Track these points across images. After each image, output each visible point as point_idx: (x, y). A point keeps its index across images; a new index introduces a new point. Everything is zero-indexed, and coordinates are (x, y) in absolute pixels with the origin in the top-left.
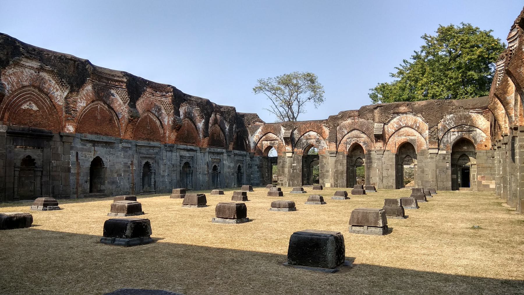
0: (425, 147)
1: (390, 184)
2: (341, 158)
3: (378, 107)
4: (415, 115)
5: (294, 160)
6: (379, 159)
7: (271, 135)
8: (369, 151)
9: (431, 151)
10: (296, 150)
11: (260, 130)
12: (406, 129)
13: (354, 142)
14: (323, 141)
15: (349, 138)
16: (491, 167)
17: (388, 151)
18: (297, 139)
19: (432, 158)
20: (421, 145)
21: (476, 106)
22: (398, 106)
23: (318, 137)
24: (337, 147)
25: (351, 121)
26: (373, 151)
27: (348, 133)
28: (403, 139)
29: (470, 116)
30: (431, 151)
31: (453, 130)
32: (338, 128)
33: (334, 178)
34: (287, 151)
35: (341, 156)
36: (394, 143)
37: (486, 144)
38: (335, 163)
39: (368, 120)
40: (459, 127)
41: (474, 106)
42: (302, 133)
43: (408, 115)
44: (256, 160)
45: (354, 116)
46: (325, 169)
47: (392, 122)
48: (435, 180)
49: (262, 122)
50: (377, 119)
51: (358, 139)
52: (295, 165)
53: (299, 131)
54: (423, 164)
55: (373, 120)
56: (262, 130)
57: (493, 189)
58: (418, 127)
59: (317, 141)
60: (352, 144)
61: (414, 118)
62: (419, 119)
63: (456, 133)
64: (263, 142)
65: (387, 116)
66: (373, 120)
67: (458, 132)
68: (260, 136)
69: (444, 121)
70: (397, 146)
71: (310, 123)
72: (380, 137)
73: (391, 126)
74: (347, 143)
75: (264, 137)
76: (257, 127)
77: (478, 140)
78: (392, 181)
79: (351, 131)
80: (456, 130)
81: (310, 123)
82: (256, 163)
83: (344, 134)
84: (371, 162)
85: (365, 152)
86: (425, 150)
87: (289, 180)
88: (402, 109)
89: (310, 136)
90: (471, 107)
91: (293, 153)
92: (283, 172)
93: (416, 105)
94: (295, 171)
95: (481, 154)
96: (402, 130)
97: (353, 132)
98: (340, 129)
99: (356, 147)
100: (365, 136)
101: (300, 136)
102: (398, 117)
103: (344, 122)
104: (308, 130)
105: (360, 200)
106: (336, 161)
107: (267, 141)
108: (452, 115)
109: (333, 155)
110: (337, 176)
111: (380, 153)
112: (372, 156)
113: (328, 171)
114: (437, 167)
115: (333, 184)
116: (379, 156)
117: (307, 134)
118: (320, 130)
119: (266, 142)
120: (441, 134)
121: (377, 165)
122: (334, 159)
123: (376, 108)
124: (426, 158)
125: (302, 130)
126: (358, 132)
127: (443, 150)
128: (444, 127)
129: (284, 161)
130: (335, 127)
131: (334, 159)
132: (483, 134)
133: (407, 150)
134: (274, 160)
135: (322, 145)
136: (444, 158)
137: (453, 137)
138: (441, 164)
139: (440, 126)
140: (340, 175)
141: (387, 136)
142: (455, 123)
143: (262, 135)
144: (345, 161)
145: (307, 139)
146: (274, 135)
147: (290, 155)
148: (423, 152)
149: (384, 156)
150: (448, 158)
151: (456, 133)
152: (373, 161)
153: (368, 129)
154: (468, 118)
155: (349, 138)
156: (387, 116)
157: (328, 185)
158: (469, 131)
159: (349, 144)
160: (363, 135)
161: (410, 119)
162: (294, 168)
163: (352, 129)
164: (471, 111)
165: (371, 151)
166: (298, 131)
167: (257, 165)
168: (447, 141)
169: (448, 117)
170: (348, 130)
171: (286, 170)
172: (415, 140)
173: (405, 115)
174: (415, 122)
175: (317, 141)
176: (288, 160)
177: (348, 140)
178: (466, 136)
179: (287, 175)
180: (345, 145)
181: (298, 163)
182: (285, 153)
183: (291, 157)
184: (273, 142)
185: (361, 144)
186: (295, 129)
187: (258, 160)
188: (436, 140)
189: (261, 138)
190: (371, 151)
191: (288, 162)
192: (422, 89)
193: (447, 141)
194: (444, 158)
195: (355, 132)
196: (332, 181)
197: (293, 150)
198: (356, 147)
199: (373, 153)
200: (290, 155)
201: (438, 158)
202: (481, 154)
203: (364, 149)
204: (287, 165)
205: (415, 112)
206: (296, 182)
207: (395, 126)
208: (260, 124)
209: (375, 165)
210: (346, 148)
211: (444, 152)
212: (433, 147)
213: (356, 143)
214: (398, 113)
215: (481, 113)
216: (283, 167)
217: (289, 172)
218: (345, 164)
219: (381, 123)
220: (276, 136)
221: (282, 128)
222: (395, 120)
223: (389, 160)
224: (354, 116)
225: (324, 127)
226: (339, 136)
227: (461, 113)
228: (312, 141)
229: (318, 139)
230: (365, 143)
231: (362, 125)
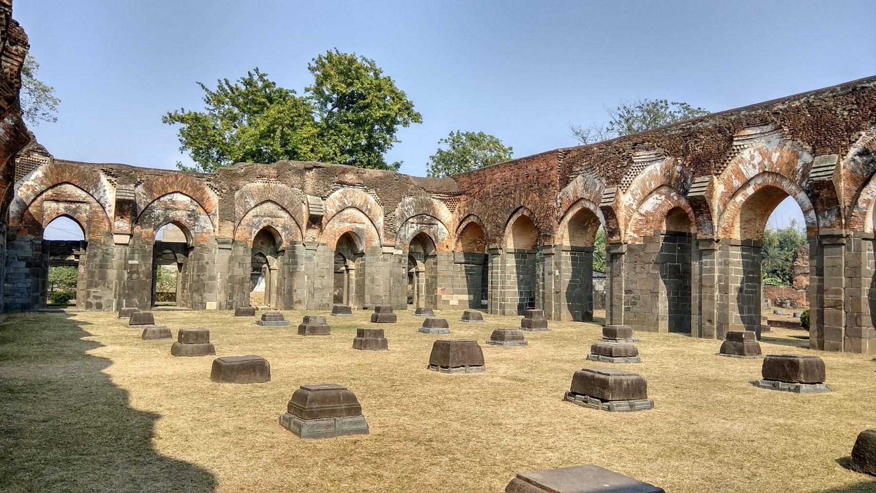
0: (376, 243)
1: (325, 301)
2: (241, 253)
3: (315, 167)
4: (366, 191)
5: (133, 252)
6: (310, 258)
7: (69, 189)
8: (293, 243)
9: (386, 250)
10: (137, 229)
11: (39, 173)
12: (352, 210)
13: (265, 224)
14: (203, 217)
15: (257, 216)
16: (452, 277)
17: (324, 244)
18: (143, 207)
19: (385, 260)
20: (371, 240)
21: (440, 190)
22: (344, 172)
23: (192, 207)
24: (234, 231)
25: (262, 184)
26: (300, 243)
27: (256, 206)
28: (346, 227)
29: (432, 203)
30: (386, 250)
31: (411, 220)
32: (237, 194)
33: (226, 292)
34: (116, 230)
35: (241, 249)
36: (335, 229)
37: (447, 244)
38: (229, 262)
39: (292, 187)
40: (420, 216)
41: (438, 189)
42: (156, 195)
43: (356, 190)
44: (22, 248)
45: (269, 177)
46: (207, 273)
47: (332, 196)
48: (388, 293)
49: (46, 154)
50: (309, 189)
51: (274, 220)
52: (136, 262)
53: (149, 189)
54: (374, 269)
55: (302, 188)
56: (46, 175)
57: (453, 307)
58: (370, 211)
59: (189, 216)
60: (261, 227)
61: (365, 194)
62: (371, 199)
63: (414, 225)
64: (46, 204)
65: (327, 186)
66: (302, 188)
67: (417, 224)
68: (38, 189)
69: (403, 206)
70: (337, 238)
71: (176, 176)
72: (315, 221)
73: (331, 204)
74: (252, 225)
75: (50, 192)
76: (33, 166)
77: (440, 238)
78: (328, 297)
79: (262, 203)
80: (415, 220)
81: (176, 176)
82: (21, 254)
83: (248, 207)
84: (296, 263)
85: (285, 245)
86: (376, 247)
87: (119, 296)
88: (350, 177)
89: (174, 202)
90: (435, 190)
91: (131, 236)
92: (103, 277)
93: (366, 175)
94: (135, 276)
95: (442, 258)
96: (346, 212)
97: (265, 206)
98: (242, 196)
99: (268, 236)
100: (286, 215)
101: (149, 201)
102: (341, 190)
103: (250, 185)
104: (170, 190)
105: (462, 332)
106: (231, 259)
107: (57, 201)
108: (411, 198)
109: (225, 246)
110: (232, 288)
111: (313, 247)
112: (297, 253)
113: (213, 278)
114: (391, 275)
115: (224, 304)
116: (309, 253)
117: (168, 197)
118: (198, 194)
119: (54, 205)
120: (398, 224)
121: (307, 269)
122: (227, 254)
123: (310, 169)
124: (378, 259)
125: (155, 189)
126: (274, 206)
127: (399, 249)
128: (403, 215)
129: (106, 255)
130: (232, 192)
131: (227, 254)
132: (445, 230)
133: (348, 243)
134: (63, 250)
135: (203, 224)
136: (400, 262)
137: (411, 230)
138: (396, 270)
139: (397, 213)
140: (237, 286)
141: (324, 220)
142: (415, 211)
143: (44, 187)
144: (248, 260)
145: (167, 209)
146: (79, 192)
147: (126, 239)
148: (374, 251)
149: (317, 253)
150: (405, 261)
151: (414, 225)
152: (299, 261)
153: (292, 203)
154: (430, 205)
155: (257, 216)
156: (327, 186)
157: (211, 305)
158: (430, 224)
159: (257, 228)
160: (282, 213)
161: (359, 195)
162: (132, 270)
163: (263, 199)
164: (434, 195)
165: (295, 243)
166: (146, 188)
167: (25, 259)
168: (405, 235)
169: (408, 200)
170: (257, 200)
171: (112, 274)
172: (363, 230)
173: (351, 188)
174: (366, 202)
175: (189, 216)
176: (116, 250)
177: (256, 220)
178: (426, 231)
179: (113, 286)
180: (248, 229)
181: (144, 258)
182: (110, 234)
183: (127, 245)
184: (73, 206)
185: (279, 229)
186: (140, 183)
187: (28, 247)
188: (391, 232)
189: (42, 193)
190: (295, 243)
191: (117, 256)
192: (308, 144)
193: (405, 235)
194: (400, 262)
195: (269, 207)
196: (221, 297)
197: (132, 229)
198: (268, 236)
199: (299, 246)
200: (126, 239)
201: (392, 260)
202: (442, 258)
203: (283, 238)
204: (116, 260)
205: (368, 185)
206: (136, 300)
207: (337, 203)
208: (41, 158)
209: (302, 268)
210: (251, 234)
211: (400, 252)
212: (389, 243)
213: (269, 227)
214: (342, 184)
215: (445, 201)
216: (103, 266)
217: (120, 277)
218: (249, 265)
219: (317, 195)
220: (84, 194)
221: (104, 178)
222: (337, 194)
223: (325, 259)
224: (269, 177)
225: (208, 189)
226: (239, 210)
227: (423, 197)
228: (179, 213)
229: (193, 211)
230: (285, 228)
231: (282, 196)
